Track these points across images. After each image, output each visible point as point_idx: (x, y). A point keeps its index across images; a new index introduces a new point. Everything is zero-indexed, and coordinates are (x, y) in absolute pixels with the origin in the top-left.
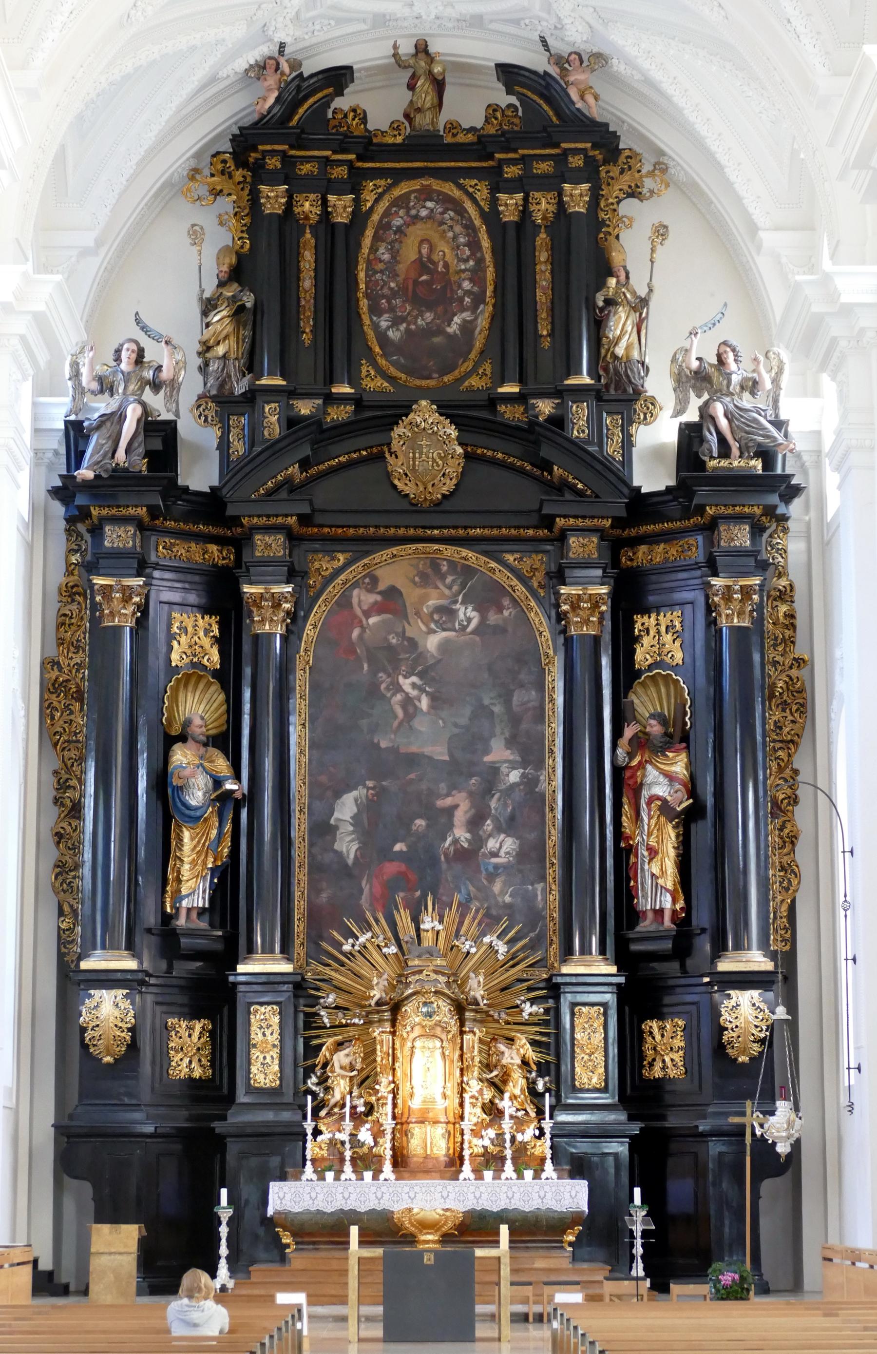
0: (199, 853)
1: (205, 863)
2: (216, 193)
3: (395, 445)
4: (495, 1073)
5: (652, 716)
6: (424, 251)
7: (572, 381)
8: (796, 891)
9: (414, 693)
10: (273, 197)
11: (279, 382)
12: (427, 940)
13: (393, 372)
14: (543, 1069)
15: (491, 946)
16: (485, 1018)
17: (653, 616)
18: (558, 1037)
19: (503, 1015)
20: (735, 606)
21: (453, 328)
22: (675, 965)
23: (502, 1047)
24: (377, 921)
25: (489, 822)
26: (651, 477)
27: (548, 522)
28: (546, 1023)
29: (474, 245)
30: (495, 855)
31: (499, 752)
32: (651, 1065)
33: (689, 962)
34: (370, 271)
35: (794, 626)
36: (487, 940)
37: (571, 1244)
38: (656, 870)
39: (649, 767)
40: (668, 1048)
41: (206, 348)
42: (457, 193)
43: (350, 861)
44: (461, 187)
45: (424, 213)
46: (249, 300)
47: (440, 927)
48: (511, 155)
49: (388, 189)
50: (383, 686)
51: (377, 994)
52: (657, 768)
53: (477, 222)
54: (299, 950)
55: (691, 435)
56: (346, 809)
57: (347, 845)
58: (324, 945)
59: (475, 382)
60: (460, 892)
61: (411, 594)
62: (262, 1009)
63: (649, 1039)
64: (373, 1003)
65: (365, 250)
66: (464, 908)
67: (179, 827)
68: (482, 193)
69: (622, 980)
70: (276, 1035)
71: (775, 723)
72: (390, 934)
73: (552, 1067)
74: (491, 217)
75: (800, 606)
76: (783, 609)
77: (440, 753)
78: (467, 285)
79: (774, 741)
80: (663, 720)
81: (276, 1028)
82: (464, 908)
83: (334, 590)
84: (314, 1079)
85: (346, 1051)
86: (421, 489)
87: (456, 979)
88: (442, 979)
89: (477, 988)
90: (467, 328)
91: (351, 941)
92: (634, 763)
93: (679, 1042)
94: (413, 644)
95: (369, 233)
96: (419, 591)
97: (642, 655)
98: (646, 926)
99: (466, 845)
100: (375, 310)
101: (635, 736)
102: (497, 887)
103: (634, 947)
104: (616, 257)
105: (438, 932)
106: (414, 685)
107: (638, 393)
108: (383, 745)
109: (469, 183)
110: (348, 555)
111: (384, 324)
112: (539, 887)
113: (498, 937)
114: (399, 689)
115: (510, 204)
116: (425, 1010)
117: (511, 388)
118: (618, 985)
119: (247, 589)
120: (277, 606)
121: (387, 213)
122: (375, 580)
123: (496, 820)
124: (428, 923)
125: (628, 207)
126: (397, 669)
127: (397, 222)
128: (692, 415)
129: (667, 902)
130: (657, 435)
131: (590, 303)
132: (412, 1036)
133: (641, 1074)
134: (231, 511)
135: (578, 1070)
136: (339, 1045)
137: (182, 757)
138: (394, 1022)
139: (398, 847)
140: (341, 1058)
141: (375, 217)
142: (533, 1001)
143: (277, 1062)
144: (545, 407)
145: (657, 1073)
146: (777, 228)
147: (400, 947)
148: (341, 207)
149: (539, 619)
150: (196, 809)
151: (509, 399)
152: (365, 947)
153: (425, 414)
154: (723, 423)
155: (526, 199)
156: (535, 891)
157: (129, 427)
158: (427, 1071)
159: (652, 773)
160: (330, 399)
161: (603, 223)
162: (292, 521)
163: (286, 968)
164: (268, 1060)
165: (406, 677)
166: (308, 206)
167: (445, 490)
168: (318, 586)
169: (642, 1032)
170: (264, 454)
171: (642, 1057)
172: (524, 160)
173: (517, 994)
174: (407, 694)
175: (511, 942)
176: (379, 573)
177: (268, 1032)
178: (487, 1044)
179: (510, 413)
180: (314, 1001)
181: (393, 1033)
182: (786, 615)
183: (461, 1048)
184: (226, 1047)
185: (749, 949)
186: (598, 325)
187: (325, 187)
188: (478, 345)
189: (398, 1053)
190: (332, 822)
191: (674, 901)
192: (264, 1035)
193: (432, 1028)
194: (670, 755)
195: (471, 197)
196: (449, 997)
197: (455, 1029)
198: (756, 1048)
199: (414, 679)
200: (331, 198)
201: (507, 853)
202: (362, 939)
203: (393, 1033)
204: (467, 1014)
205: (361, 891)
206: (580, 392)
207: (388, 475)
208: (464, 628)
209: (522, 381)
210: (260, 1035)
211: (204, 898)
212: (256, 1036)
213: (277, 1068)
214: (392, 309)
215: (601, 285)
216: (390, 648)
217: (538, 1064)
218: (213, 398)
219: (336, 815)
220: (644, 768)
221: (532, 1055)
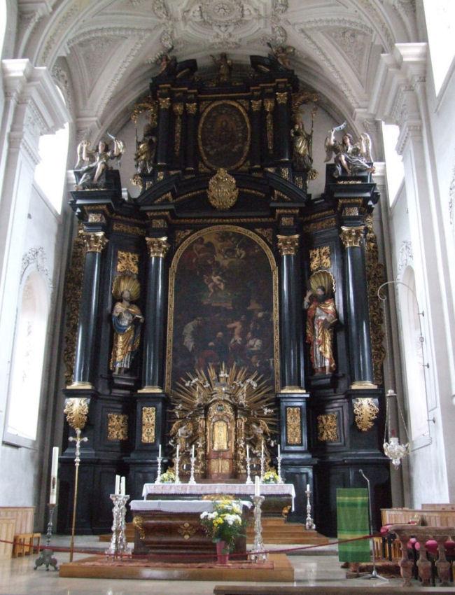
0: (125, 346)
1: (127, 349)
2: (145, 109)
3: (211, 186)
4: (252, 437)
5: (319, 287)
6: (224, 124)
8: (384, 359)
9: (218, 283)
12: (222, 381)
13: (210, 165)
14: (274, 437)
15: (250, 384)
16: (247, 414)
17: (318, 250)
18: (279, 422)
19: (256, 413)
20: (353, 239)
22: (332, 390)
23: (255, 426)
24: (201, 374)
25: (249, 333)
27: (273, 214)
28: (275, 417)
29: (243, 121)
30: (252, 347)
31: (254, 306)
32: (322, 434)
33: (338, 390)
35: (377, 252)
36: (248, 381)
37: (286, 514)
38: (320, 349)
39: (318, 309)
40: (331, 428)
41: (138, 157)
42: (236, 105)
43: (190, 350)
44: (238, 102)
45: (224, 112)
46: (154, 139)
47: (227, 376)
48: (256, 88)
49: (210, 104)
50: (205, 280)
51: (198, 401)
52: (321, 309)
54: (167, 387)
55: (330, 169)
56: (190, 327)
57: (189, 343)
58: (178, 383)
59: (245, 168)
60: (237, 361)
61: (218, 245)
62: (148, 409)
63: (321, 424)
64: (196, 406)
65: (201, 125)
66: (238, 369)
67: (117, 334)
68: (245, 104)
69: (308, 396)
70: (154, 420)
71: (372, 290)
72: (206, 379)
73: (278, 436)
74: (250, 112)
75: (379, 242)
76: (372, 244)
77: (229, 306)
78: (240, 135)
79: (371, 297)
80: (323, 289)
81: (154, 417)
82: (238, 369)
83: (185, 245)
84: (172, 441)
85: (183, 427)
86: (221, 204)
87: (233, 395)
88: (228, 396)
89: (243, 400)
91: (189, 382)
92: (312, 306)
93: (334, 424)
94: (217, 264)
95: (202, 120)
96: (219, 244)
97: (314, 265)
98: (316, 374)
99: (239, 343)
100: (205, 145)
101: (311, 296)
102: (254, 359)
103: (313, 383)
105: (227, 378)
106: (218, 280)
107: (309, 169)
108: (205, 303)
109: (240, 101)
110: (191, 231)
111: (208, 149)
112: (271, 360)
113: (254, 380)
114: (212, 281)
115: (256, 105)
116: (219, 408)
118: (306, 398)
119: (147, 239)
120: (160, 246)
122: (202, 239)
123: (253, 333)
124: (222, 375)
126: (211, 273)
127: (214, 115)
128: (332, 162)
129: (327, 363)
132: (214, 420)
133: (317, 439)
134: (143, 208)
135: (289, 436)
136: (181, 426)
137: (120, 308)
138: (206, 414)
139: (211, 344)
140: (181, 431)
141: (205, 114)
142: (269, 407)
143: (153, 432)
145: (324, 437)
146: (360, 107)
147: (210, 383)
148: (192, 107)
149: (269, 253)
150: (124, 326)
152: (195, 385)
153: (222, 172)
154: (344, 162)
155: (263, 103)
156: (270, 361)
158: (221, 437)
159: (318, 311)
160: (185, 173)
161: (293, 113)
163: (159, 391)
164: (150, 431)
165: (215, 276)
166: (178, 108)
167: (231, 204)
168: (179, 242)
169: (317, 421)
171: (318, 431)
172: (263, 89)
173: (262, 405)
174: (215, 283)
175: (259, 383)
176: (204, 237)
177: (150, 419)
178: (247, 426)
180: (173, 407)
181: (206, 419)
182: (374, 247)
183: (236, 426)
184: (133, 426)
185: (365, 379)
187: (184, 100)
188: (245, 154)
189: (208, 429)
190: (183, 334)
191: (330, 364)
192: (148, 420)
193: (222, 417)
194: (327, 303)
195: (243, 106)
196: (230, 403)
197: (233, 417)
198: (371, 424)
199: (218, 277)
200: (187, 104)
201: (257, 346)
202: (194, 381)
203: (206, 419)
204: (239, 411)
205: (194, 361)
208: (239, 257)
210: (146, 421)
211: (127, 364)
212: (145, 420)
213: (153, 434)
214: (211, 144)
216: (209, 265)
217: (271, 434)
218: (140, 175)
219: (185, 331)
220: (315, 309)
221: (268, 429)
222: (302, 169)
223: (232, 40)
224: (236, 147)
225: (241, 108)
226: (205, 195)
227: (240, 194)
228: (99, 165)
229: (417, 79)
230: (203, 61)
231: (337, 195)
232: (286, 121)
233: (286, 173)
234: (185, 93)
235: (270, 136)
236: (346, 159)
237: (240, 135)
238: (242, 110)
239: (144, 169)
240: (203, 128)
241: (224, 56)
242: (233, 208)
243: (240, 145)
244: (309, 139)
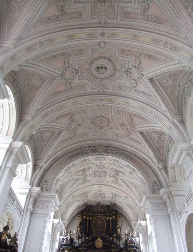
2: (79, 217)
3: (96, 242)
7: (114, 236)
10: (84, 217)
11: (84, 235)
13: (96, 235)
21: (102, 230)
26: (122, 246)
34: (94, 225)
41: (77, 232)
42: (102, 217)
46: (82, 227)
53: (104, 220)
55: (126, 241)
59: (104, 236)
74: (106, 219)
78: (103, 226)
90: (103, 230)
95: (94, 221)
104: (118, 223)
107: (121, 237)
117: (107, 236)
121: (96, 219)
125: (119, 219)
127: (96, 220)
128: (126, 239)
130: (123, 241)
131: (116, 228)
141: (94, 219)
144: (111, 238)
146: (133, 221)
148: (91, 218)
151: (107, 237)
154: (129, 239)
155: (109, 218)
157: (69, 239)
162: (85, 250)
166: (88, 218)
170: (83, 243)
172: (109, 214)
179: (108, 239)
186: (116, 230)
187: (89, 216)
188: (104, 232)
206: (115, 237)
207: (95, 246)
209: (109, 236)
215: (117, 226)
222: (119, 237)
223: (101, 200)
224: (102, 230)
225: (103, 218)
226: (94, 244)
227: (104, 245)
228: (69, 237)
229: (145, 229)
230: (94, 204)
231: (127, 248)
232: (115, 223)
233: (115, 239)
234: (89, 214)
235: (111, 227)
236: (130, 239)
237: (103, 226)
238: (104, 219)
239: (79, 236)
240: (94, 224)
241: (99, 203)
242: (101, 248)
243: (103, 229)
244: (120, 228)
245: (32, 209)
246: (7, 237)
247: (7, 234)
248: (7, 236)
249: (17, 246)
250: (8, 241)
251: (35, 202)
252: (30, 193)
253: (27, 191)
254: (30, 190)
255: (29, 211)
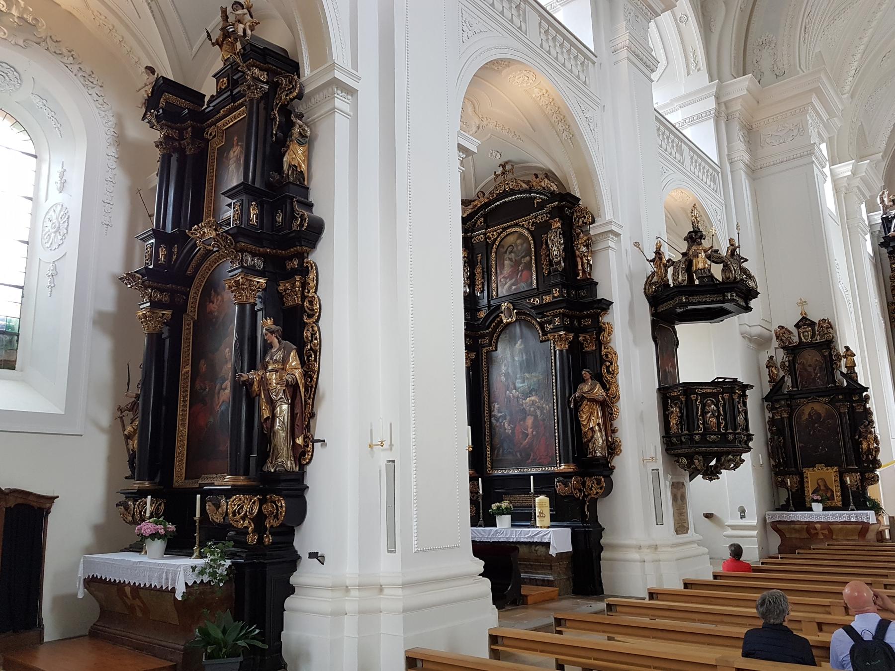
245: (746, 157)
246: (709, 262)
247: (705, 251)
248: (709, 257)
249: (750, 276)
250: (717, 271)
251: (751, 133)
252: (723, 108)
253: (710, 104)
254: (717, 98)
255: (742, 165)
